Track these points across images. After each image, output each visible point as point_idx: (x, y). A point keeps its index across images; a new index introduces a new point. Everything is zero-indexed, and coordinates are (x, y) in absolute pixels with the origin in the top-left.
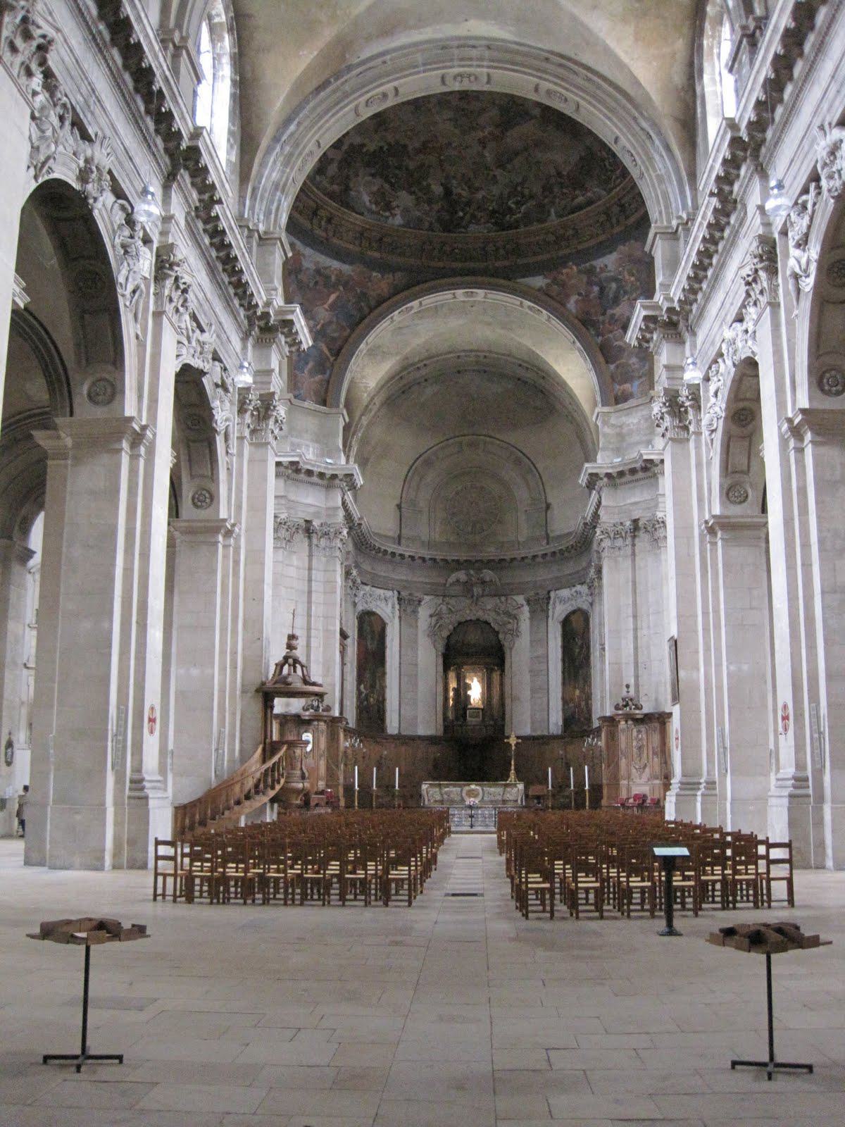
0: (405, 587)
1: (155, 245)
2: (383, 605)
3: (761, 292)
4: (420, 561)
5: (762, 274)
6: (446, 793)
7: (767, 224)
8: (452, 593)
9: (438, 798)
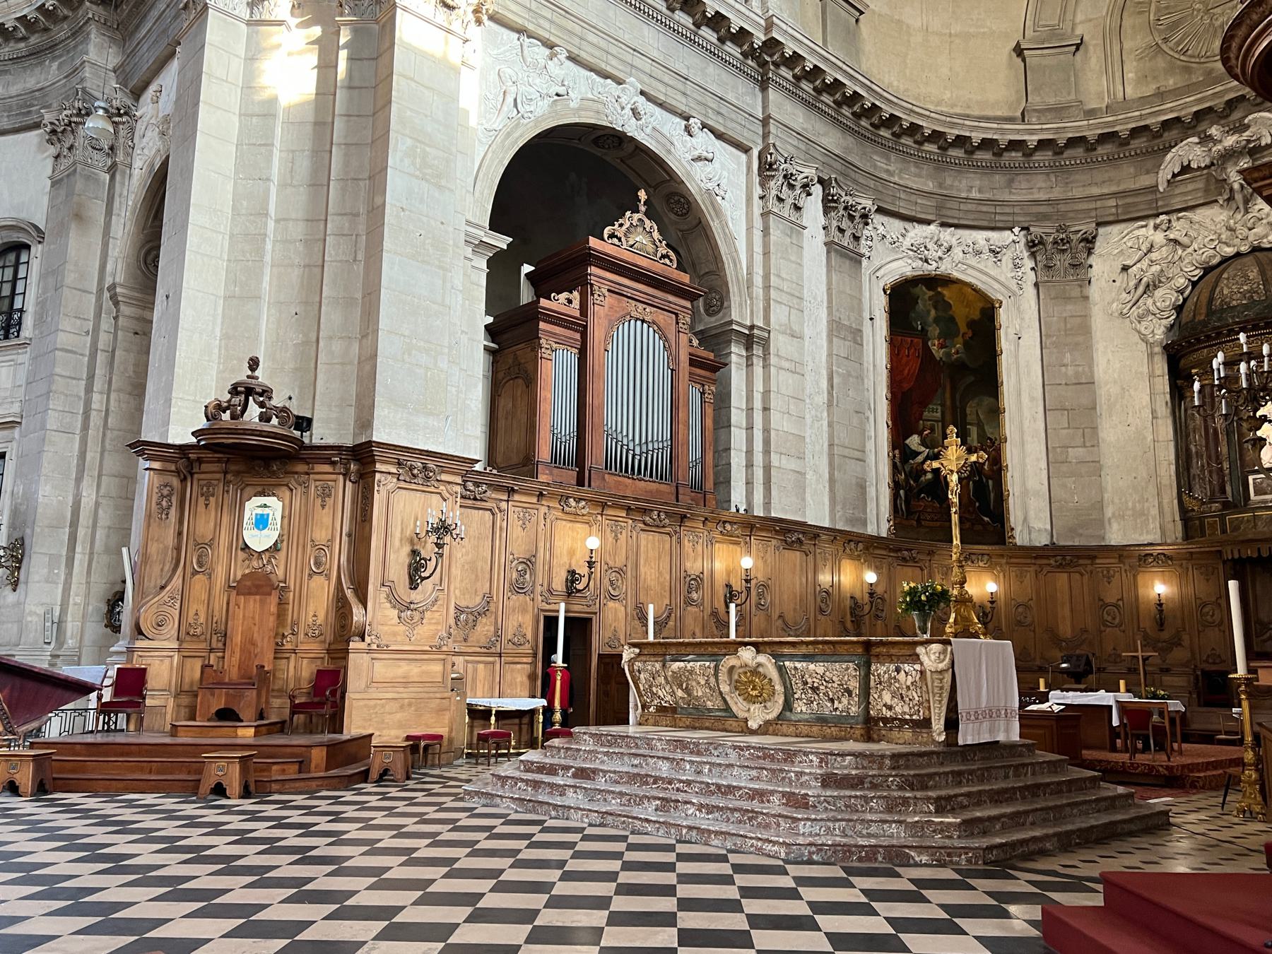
0: (1043, 217)
2: (987, 262)
4: (1079, 152)
6: (678, 680)
8: (1177, 203)
9: (665, 695)
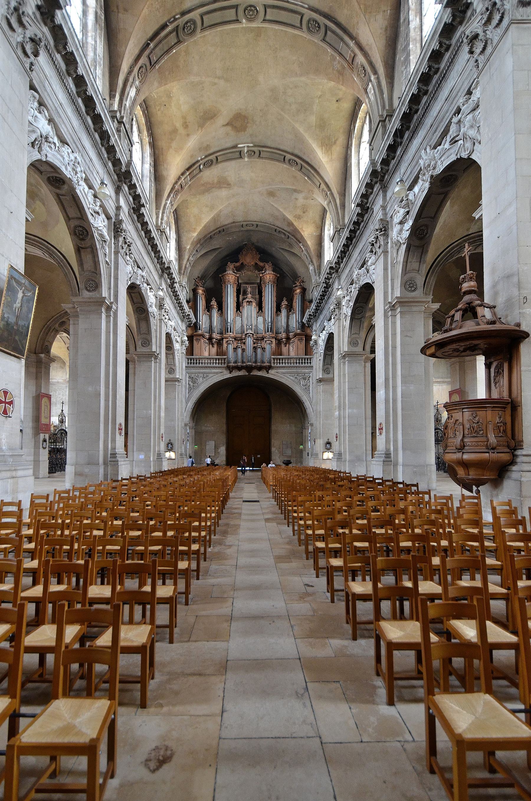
1: (113, 220)
3: (379, 247)
5: (381, 239)
7: (385, 214)
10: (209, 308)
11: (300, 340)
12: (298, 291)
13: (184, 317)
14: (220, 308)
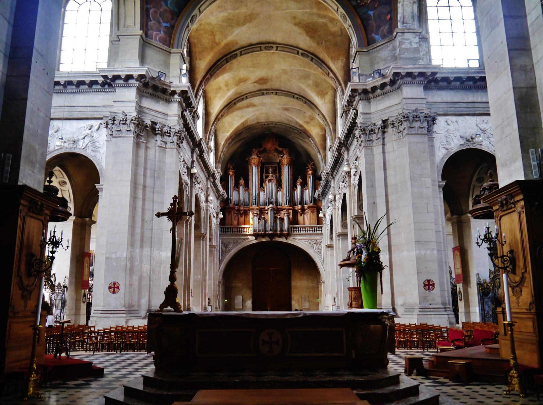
10: (237, 186)
11: (313, 212)
12: (310, 172)
13: (218, 196)
14: (247, 186)
